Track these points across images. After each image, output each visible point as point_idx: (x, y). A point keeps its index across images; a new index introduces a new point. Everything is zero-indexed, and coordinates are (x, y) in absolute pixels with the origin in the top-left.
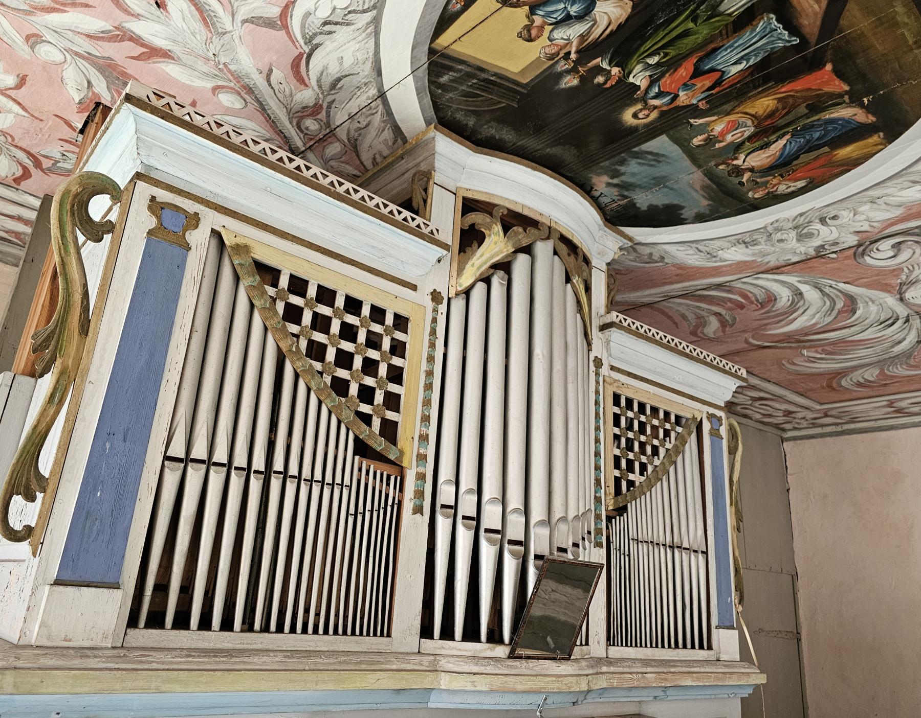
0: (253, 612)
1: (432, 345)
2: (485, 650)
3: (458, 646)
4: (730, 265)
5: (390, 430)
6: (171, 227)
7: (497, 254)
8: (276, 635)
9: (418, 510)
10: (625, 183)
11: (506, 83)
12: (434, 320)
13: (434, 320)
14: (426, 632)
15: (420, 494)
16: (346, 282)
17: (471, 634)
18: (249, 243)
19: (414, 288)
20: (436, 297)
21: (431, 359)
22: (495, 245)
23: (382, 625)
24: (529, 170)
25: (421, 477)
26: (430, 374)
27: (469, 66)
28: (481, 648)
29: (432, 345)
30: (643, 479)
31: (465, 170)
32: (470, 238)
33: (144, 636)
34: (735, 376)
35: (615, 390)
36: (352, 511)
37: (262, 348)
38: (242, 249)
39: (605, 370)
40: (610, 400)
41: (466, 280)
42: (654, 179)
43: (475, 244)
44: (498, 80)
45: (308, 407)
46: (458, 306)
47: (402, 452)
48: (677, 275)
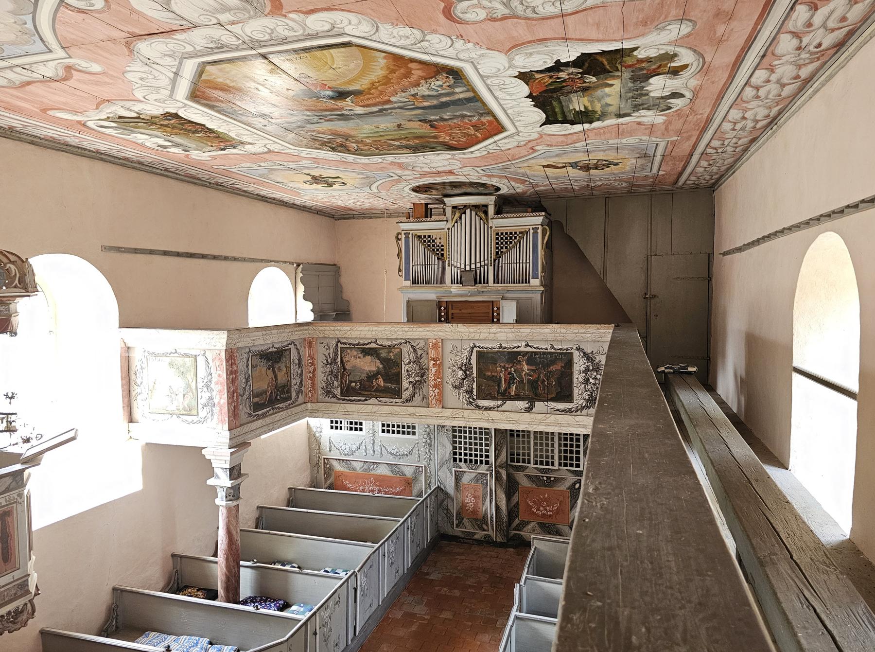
5: (442, 255)
6: (407, 235)
22: (457, 215)
23: (445, 283)
39: (494, 228)
45: (428, 253)
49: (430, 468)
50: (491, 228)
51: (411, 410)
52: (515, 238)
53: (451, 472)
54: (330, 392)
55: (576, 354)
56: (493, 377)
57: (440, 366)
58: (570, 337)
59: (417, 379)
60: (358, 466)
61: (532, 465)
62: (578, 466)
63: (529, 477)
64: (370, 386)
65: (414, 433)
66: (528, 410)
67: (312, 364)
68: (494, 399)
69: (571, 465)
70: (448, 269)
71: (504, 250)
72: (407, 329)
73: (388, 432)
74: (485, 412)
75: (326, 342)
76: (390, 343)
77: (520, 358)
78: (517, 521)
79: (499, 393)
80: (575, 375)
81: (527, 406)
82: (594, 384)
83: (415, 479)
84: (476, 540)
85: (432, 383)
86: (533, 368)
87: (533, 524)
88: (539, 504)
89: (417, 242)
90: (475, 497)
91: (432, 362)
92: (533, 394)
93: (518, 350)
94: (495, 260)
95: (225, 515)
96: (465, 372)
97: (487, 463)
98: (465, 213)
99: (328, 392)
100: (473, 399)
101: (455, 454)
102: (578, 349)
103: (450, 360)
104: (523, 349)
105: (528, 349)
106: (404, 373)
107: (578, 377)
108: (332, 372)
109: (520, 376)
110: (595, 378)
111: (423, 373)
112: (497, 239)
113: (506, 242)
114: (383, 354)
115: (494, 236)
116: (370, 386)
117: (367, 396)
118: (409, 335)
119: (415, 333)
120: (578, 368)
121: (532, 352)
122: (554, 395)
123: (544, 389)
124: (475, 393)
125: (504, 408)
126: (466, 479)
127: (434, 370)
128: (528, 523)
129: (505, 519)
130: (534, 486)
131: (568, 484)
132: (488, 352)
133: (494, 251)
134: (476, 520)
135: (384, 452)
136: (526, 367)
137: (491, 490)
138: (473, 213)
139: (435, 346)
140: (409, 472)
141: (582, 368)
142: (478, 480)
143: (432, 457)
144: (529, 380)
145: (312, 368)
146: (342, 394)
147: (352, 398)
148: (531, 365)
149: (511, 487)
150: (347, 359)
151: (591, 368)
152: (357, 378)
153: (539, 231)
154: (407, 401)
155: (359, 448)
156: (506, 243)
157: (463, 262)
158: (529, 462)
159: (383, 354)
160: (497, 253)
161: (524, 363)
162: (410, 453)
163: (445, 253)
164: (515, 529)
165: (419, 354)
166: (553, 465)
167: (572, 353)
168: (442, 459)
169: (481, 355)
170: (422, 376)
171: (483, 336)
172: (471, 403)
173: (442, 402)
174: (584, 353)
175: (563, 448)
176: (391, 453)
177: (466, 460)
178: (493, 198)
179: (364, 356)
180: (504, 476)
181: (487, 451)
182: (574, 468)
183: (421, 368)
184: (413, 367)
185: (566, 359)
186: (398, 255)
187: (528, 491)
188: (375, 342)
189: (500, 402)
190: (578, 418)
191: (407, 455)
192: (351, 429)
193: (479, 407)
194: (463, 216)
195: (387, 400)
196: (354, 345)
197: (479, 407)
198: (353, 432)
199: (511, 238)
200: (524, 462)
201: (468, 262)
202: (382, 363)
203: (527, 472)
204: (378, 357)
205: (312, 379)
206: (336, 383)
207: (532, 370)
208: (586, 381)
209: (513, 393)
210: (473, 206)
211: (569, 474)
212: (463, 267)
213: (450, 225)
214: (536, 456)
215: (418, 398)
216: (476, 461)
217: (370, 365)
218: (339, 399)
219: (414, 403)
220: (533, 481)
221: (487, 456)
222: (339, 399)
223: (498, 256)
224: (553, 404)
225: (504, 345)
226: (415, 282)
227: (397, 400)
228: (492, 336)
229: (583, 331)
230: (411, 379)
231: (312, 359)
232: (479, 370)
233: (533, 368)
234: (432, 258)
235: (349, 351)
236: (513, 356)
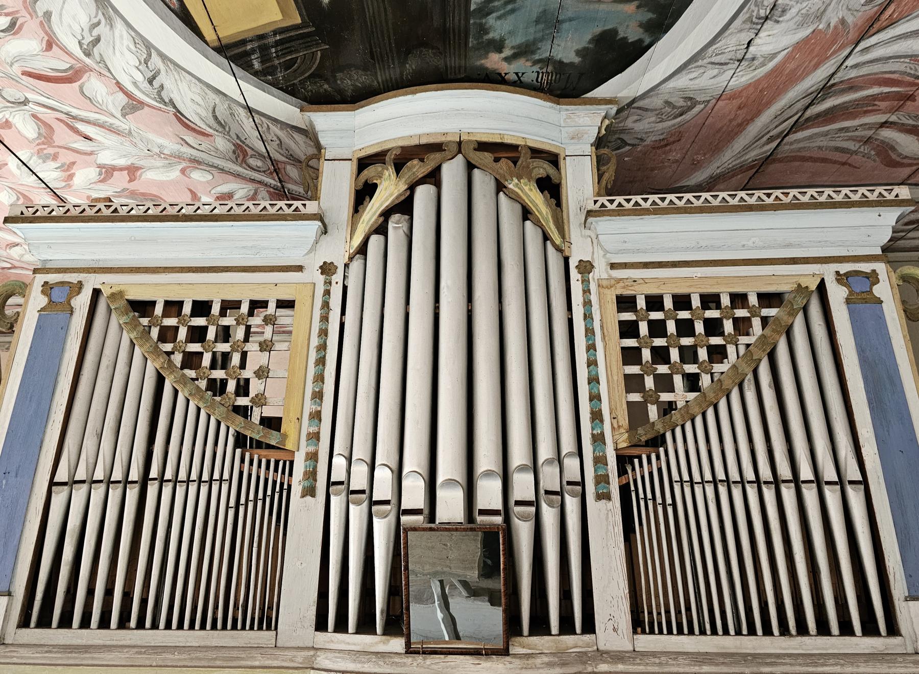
1: (325, 319)
2: (376, 643)
3: (353, 641)
4: (789, 58)
7: (387, 199)
8: (151, 631)
9: (310, 491)
10: (519, 46)
11: (293, 34)
12: (327, 293)
13: (327, 293)
14: (321, 625)
15: (311, 475)
17: (366, 625)
18: (122, 288)
19: (299, 268)
20: (327, 269)
21: (324, 333)
22: (389, 189)
24: (410, 97)
25: (313, 457)
26: (323, 347)
27: (251, 41)
29: (325, 319)
30: (692, 396)
34: (882, 203)
35: (619, 292)
36: (232, 503)
39: (600, 271)
40: (612, 306)
42: (537, 22)
43: (367, 199)
44: (283, 36)
47: (285, 437)
48: (739, 108)
50: (586, 267)
52: (742, 326)
70: (304, 515)
71: (680, 395)
89: (115, 333)
94: (624, 461)
98: (434, 178)
115: (608, 317)
133: (614, 400)
138: (483, 182)
153: (884, 290)
157: (415, 459)
160: (636, 413)
201: (449, 465)
212: (414, 494)
213: (337, 249)
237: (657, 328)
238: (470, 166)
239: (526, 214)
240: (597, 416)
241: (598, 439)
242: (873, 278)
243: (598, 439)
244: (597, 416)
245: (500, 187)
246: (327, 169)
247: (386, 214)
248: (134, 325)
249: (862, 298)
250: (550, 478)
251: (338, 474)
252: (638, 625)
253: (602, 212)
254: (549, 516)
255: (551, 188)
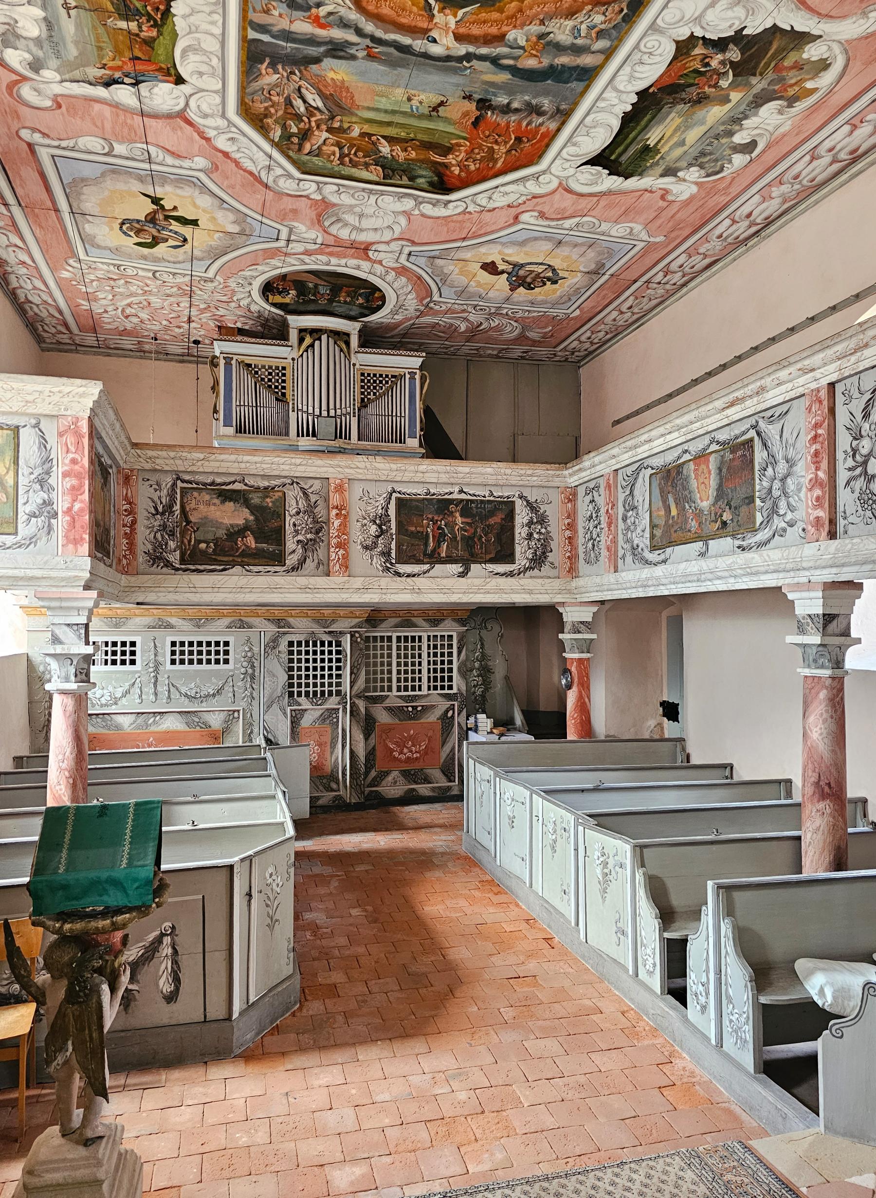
0: (258, 431)
3: (305, 438)
5: (284, 394)
6: (228, 361)
9: (293, 411)
14: (298, 436)
15: (293, 408)
16: (267, 362)
17: (308, 435)
20: (293, 359)
22: (308, 341)
23: (287, 434)
28: (310, 438)
31: (297, 322)
32: (301, 340)
33: (238, 434)
37: (251, 382)
38: (243, 362)
39: (357, 366)
41: (301, 353)
46: (300, 359)
49: (251, 710)
50: (354, 365)
51: (302, 581)
52: (387, 382)
53: (285, 714)
54: (160, 558)
55: (519, 505)
56: (418, 531)
57: (345, 518)
58: (514, 480)
59: (309, 536)
60: (125, 721)
61: (395, 692)
62: (450, 687)
63: (389, 709)
64: (232, 548)
65: (226, 662)
66: (462, 575)
67: (130, 512)
68: (419, 562)
69: (443, 688)
70: (293, 416)
71: (372, 397)
72: (298, 461)
73: (182, 662)
74: (409, 579)
75: (154, 478)
76: (266, 484)
77: (452, 507)
78: (373, 774)
79: (425, 555)
80: (517, 530)
81: (461, 570)
82: (539, 540)
83: (226, 730)
84: (321, 807)
85: (334, 541)
86: (469, 520)
87: (395, 774)
88: (401, 745)
89: (244, 373)
90: (320, 745)
91: (334, 512)
92: (468, 555)
93: (450, 497)
94: (359, 410)
95: (70, 708)
96: (380, 526)
97: (338, 693)
98: (320, 339)
99: (157, 558)
100: (391, 564)
101: (291, 685)
102: (521, 497)
103: (357, 510)
104: (456, 496)
105: (463, 496)
106: (289, 529)
107: (520, 532)
108: (164, 527)
109: (452, 531)
110: (540, 533)
111: (319, 528)
112: (362, 381)
113: (374, 386)
114: (256, 500)
115: (358, 378)
116: (232, 548)
117: (227, 563)
118: (300, 471)
119: (309, 469)
120: (520, 521)
121: (468, 501)
122: (492, 555)
123: (481, 548)
124: (393, 555)
125: (431, 573)
126: (306, 721)
127: (337, 523)
128: (387, 773)
129: (363, 770)
130: (397, 721)
131: (438, 712)
132: (411, 500)
133: (358, 397)
134: (320, 777)
135: (175, 695)
136: (459, 520)
137: (344, 730)
139: (340, 489)
140: (216, 721)
141: (525, 521)
142: (324, 720)
143: (255, 694)
144: (463, 538)
145: (130, 519)
146: (183, 561)
147: (201, 567)
148: (466, 517)
149: (368, 725)
150: (193, 505)
151: (535, 520)
152: (210, 537)
153: (417, 377)
154: (293, 569)
155: (127, 692)
156: (375, 388)
158: (390, 689)
159: (256, 500)
160: (363, 400)
161: (458, 514)
162: (219, 692)
163: (289, 392)
164: (368, 787)
165: (313, 500)
166: (420, 690)
167: (513, 502)
168: (270, 696)
169: (402, 504)
170: (317, 533)
171: (407, 476)
172: (388, 569)
173: (345, 566)
174: (528, 501)
175: (432, 667)
176: (186, 695)
177: (307, 694)
178: (357, 325)
179: (223, 502)
180: (363, 710)
181: (339, 676)
182: (446, 691)
183: (315, 521)
184: (304, 520)
185: (508, 508)
186: (213, 388)
187: (388, 729)
188: (243, 481)
189: (427, 567)
190: (522, 582)
191: (214, 695)
192: (114, 662)
193: (398, 574)
194: (317, 343)
195: (260, 568)
196: (205, 484)
197: (398, 574)
198: (118, 667)
199: (381, 382)
200: (382, 690)
201: (324, 407)
202: (252, 513)
203: (388, 703)
204: (247, 503)
205: (130, 537)
206: (172, 544)
207: (467, 523)
208: (530, 536)
209: (443, 555)
210: (331, 331)
211: (440, 699)
213: (295, 354)
214: (399, 680)
215: (310, 565)
216: (323, 693)
217: (233, 516)
218: (177, 569)
219: (303, 572)
220: (395, 715)
221: (338, 684)
222: (177, 569)
223: (364, 404)
224: (491, 567)
225: (432, 491)
226: (240, 430)
227: (277, 568)
228: (419, 477)
229: (529, 472)
230: (300, 537)
231: (130, 503)
232: (399, 524)
233: (469, 520)
234: (266, 397)
235: (195, 494)
236: (443, 505)
237: (369, 381)
238: (328, 337)
239: (341, 350)
240: (354, 400)
241: (354, 405)
242: (415, 373)
243: (354, 405)
244: (354, 400)
245: (335, 343)
246: (291, 330)
247: (308, 347)
248: (248, 370)
249: (412, 379)
250: (344, 411)
251: (300, 407)
252: (359, 440)
253: (359, 352)
254: (343, 418)
255: (348, 344)
